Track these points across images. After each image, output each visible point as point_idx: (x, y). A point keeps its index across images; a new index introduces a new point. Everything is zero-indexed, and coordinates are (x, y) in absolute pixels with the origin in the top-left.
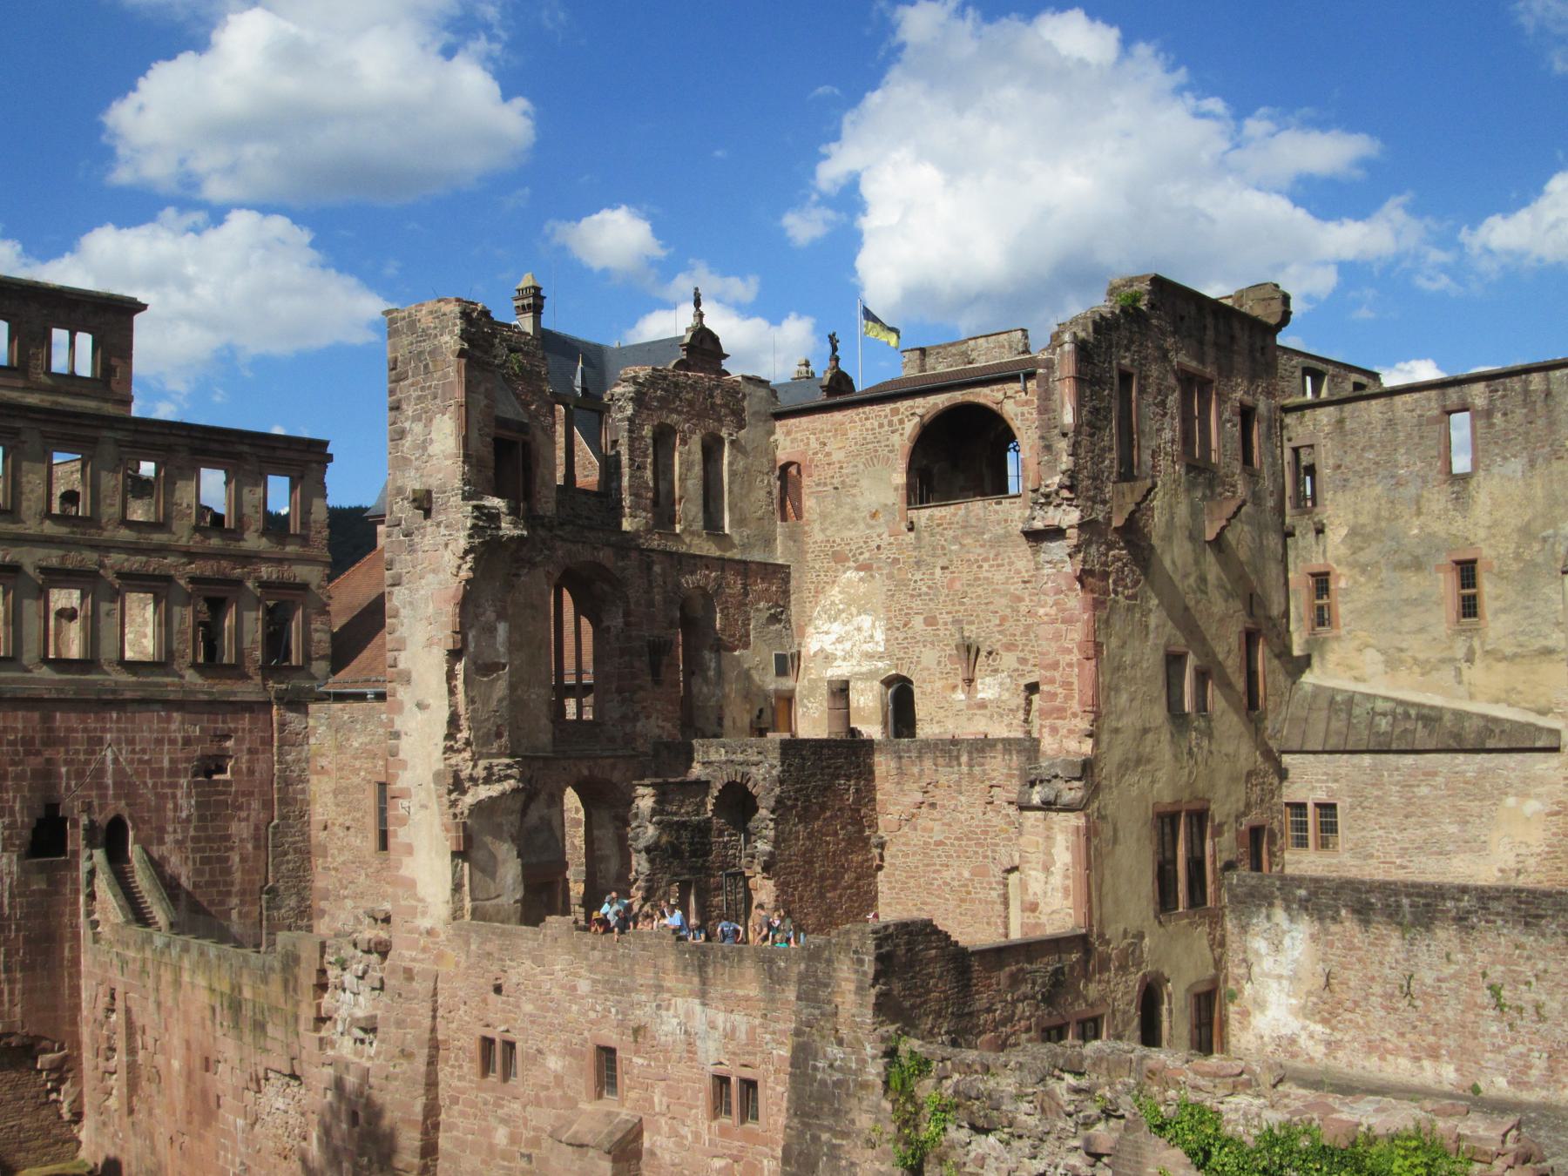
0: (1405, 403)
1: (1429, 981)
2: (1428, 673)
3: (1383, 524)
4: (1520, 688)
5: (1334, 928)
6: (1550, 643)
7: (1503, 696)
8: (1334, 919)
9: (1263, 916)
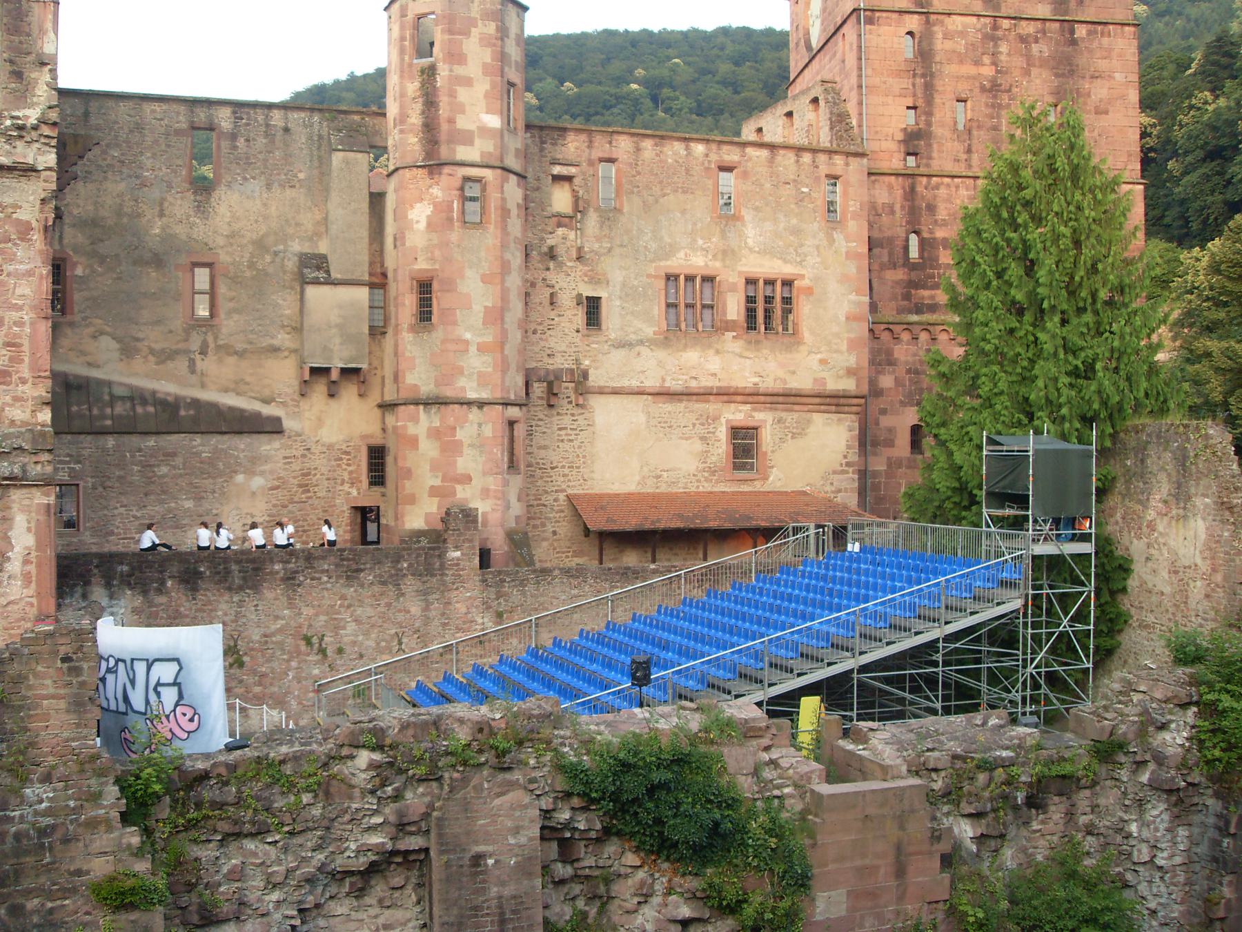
0: (153, 111)
1: (256, 638)
2: (163, 362)
3: (125, 220)
4: (248, 379)
5: (162, 599)
6: (276, 342)
7: (232, 386)
8: (160, 591)
9: (77, 595)
